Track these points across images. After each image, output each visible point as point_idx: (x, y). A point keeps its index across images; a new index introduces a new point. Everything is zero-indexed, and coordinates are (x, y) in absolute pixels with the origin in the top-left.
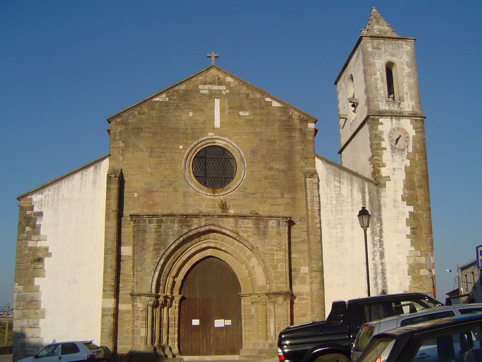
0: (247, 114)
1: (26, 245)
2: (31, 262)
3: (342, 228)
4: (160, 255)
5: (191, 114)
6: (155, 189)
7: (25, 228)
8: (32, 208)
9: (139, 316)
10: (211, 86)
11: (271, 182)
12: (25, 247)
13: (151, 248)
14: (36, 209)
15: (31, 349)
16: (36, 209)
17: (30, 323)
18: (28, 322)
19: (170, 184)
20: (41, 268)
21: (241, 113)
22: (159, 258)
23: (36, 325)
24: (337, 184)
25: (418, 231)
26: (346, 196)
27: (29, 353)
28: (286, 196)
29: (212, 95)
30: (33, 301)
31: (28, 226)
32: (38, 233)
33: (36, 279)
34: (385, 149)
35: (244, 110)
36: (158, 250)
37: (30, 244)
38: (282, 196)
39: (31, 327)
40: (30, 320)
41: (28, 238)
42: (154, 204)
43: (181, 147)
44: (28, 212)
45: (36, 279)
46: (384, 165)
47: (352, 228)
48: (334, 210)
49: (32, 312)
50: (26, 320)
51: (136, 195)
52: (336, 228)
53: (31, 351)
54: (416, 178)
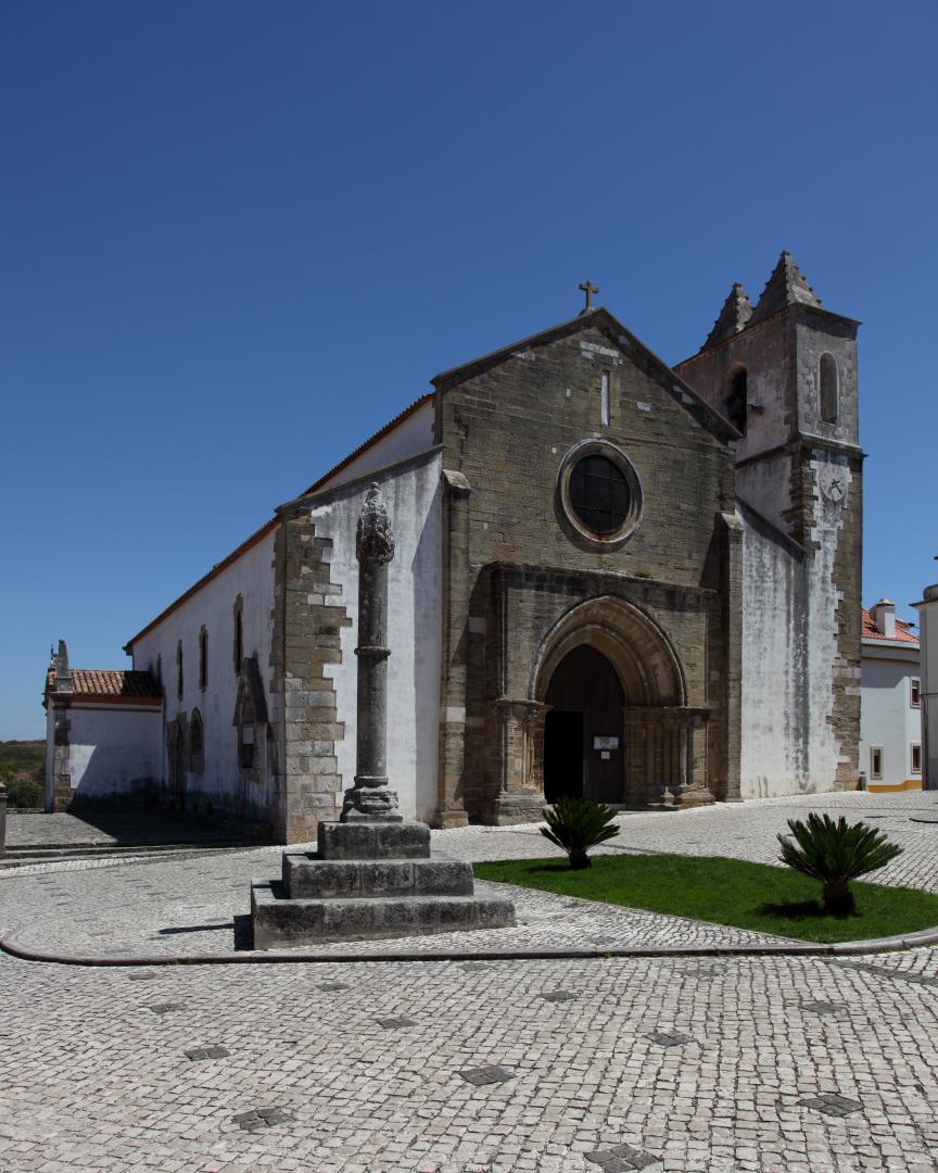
0: (648, 409)
1: (304, 601)
2: (316, 634)
3: (762, 615)
4: (542, 637)
5: (568, 393)
6: (515, 520)
7: (300, 569)
8: (310, 529)
9: (512, 738)
10: (597, 347)
11: (675, 532)
12: (301, 604)
13: (529, 625)
14: (318, 533)
15: (320, 796)
16: (318, 533)
17: (317, 748)
18: (313, 746)
19: (538, 515)
20: (333, 647)
21: (641, 405)
22: (540, 642)
23: (328, 751)
24: (758, 546)
25: (847, 628)
26: (768, 565)
27: (317, 803)
28: (695, 556)
29: (602, 364)
30: (323, 707)
31: (305, 564)
32: (325, 579)
33: (326, 667)
34: (816, 498)
35: (644, 400)
36: (537, 628)
37: (312, 599)
38: (690, 557)
39: (318, 756)
40: (316, 742)
41: (308, 590)
42: (513, 547)
43: (554, 450)
44: (305, 538)
45: (326, 667)
46: (814, 524)
47: (774, 617)
48: (753, 585)
49: (320, 728)
50: (309, 743)
51: (486, 526)
52: (755, 615)
53: (319, 800)
54: (850, 549)
